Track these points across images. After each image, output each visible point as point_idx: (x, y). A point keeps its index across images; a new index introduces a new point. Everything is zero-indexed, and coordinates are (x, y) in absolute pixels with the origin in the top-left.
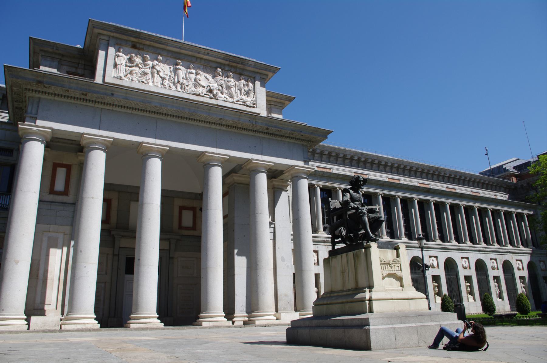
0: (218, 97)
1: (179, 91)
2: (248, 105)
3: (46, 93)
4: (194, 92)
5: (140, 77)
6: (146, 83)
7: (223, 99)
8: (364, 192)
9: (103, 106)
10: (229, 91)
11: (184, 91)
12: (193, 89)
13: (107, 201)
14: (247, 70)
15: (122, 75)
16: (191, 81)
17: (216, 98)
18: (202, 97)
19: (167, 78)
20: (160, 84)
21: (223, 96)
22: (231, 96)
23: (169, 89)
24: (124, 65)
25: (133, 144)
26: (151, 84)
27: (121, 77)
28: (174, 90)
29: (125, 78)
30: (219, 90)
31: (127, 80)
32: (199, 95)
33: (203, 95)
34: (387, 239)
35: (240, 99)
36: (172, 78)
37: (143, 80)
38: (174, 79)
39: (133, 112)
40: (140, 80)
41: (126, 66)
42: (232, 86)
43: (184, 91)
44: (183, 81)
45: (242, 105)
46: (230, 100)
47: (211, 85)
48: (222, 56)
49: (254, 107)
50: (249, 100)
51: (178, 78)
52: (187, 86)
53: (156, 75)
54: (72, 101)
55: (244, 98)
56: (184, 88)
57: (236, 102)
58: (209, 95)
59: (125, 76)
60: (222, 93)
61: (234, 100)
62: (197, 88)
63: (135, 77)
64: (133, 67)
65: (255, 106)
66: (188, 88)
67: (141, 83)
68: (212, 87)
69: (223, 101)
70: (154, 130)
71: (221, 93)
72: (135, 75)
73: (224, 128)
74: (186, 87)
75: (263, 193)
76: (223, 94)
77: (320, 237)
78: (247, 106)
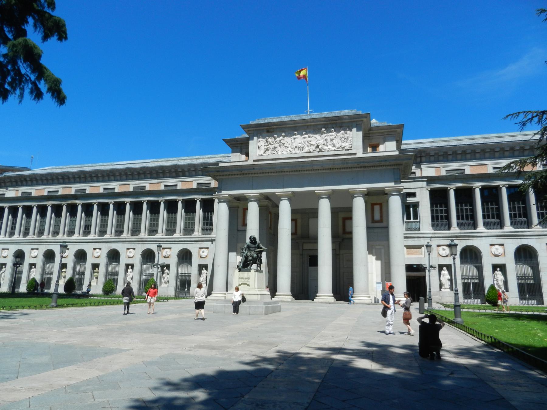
2: (346, 149)
3: (224, 175)
5: (272, 151)
7: (327, 150)
8: (507, 186)
9: (252, 175)
13: (293, 220)
14: (345, 122)
15: (262, 153)
16: (305, 143)
18: (312, 153)
22: (334, 146)
23: (290, 153)
26: (280, 153)
27: (262, 154)
29: (264, 154)
30: (324, 144)
31: (266, 155)
32: (310, 152)
33: (313, 151)
34: (539, 228)
40: (273, 153)
42: (334, 139)
45: (342, 150)
46: (333, 149)
47: (317, 142)
48: (324, 119)
49: (351, 149)
50: (347, 145)
52: (302, 148)
53: (282, 146)
54: (237, 176)
55: (344, 145)
56: (300, 150)
59: (264, 153)
60: (327, 146)
63: (269, 152)
64: (269, 145)
67: (274, 154)
68: (319, 143)
71: (326, 146)
73: (328, 171)
74: (301, 149)
75: (359, 212)
77: (451, 233)
78: (346, 150)
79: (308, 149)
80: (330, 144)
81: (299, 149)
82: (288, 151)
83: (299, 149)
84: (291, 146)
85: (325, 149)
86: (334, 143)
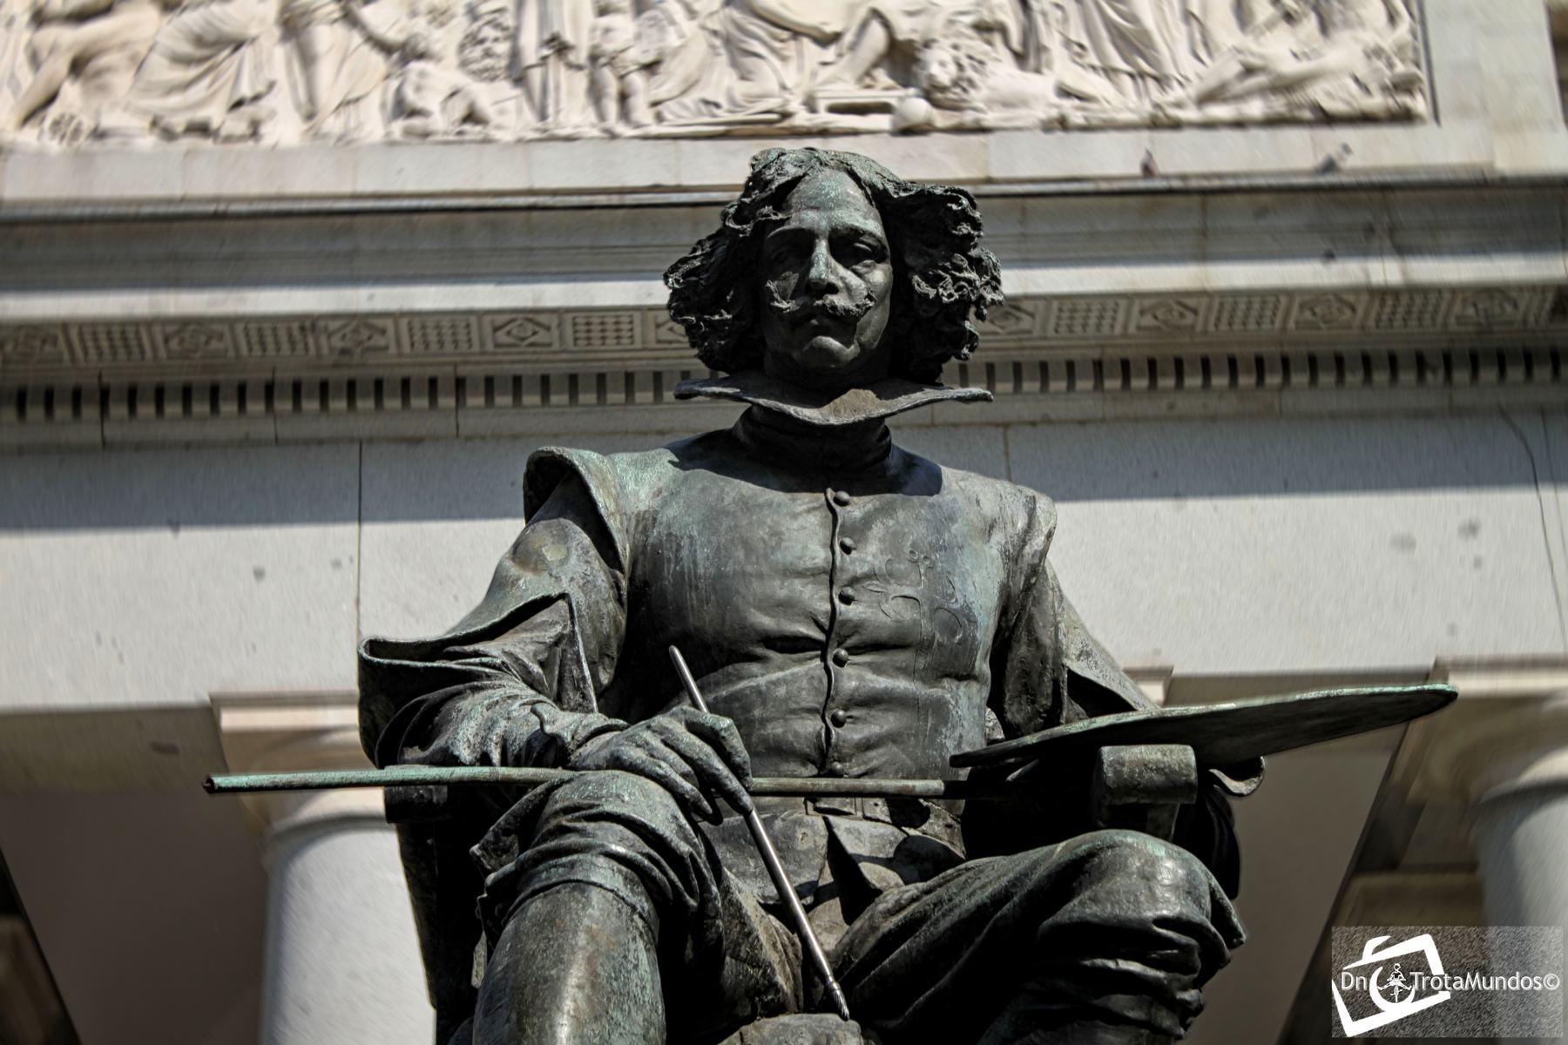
0: (991, 102)
1: (569, 139)
2: (1330, 105)
4: (724, 115)
6: (229, 139)
7: (1054, 113)
10: (1110, 25)
11: (622, 129)
12: (722, 83)
17: (968, 117)
19: (444, 40)
20: (383, 105)
21: (1039, 87)
24: (24, 18)
25: (159, 748)
26: (284, 129)
28: (520, 141)
29: (29, 137)
31: (54, 146)
33: (823, 118)
35: (1236, 68)
36: (489, 32)
37: (200, 115)
38: (514, 36)
39: (113, 432)
41: (40, 18)
43: (622, 129)
44: (607, 31)
45: (1272, 122)
49: (1405, 117)
51: (544, 19)
52: (650, 68)
56: (624, 98)
57: (1190, 114)
58: (884, 108)
59: (32, 115)
60: (1027, 55)
61: (1176, 93)
62: (750, 62)
65: (1419, 104)
66: (661, 94)
67: (187, 142)
69: (1048, 127)
70: (337, 564)
71: (1020, 58)
72: (122, 81)
73: (1084, 400)
74: (637, 80)
76: (1038, 71)
78: (1327, 119)
79: (741, 89)
80: (1078, 34)
81: (595, 93)
82: (431, 101)
83: (609, 78)
84: (474, 40)
85: (1007, 104)
86: (1149, 20)
